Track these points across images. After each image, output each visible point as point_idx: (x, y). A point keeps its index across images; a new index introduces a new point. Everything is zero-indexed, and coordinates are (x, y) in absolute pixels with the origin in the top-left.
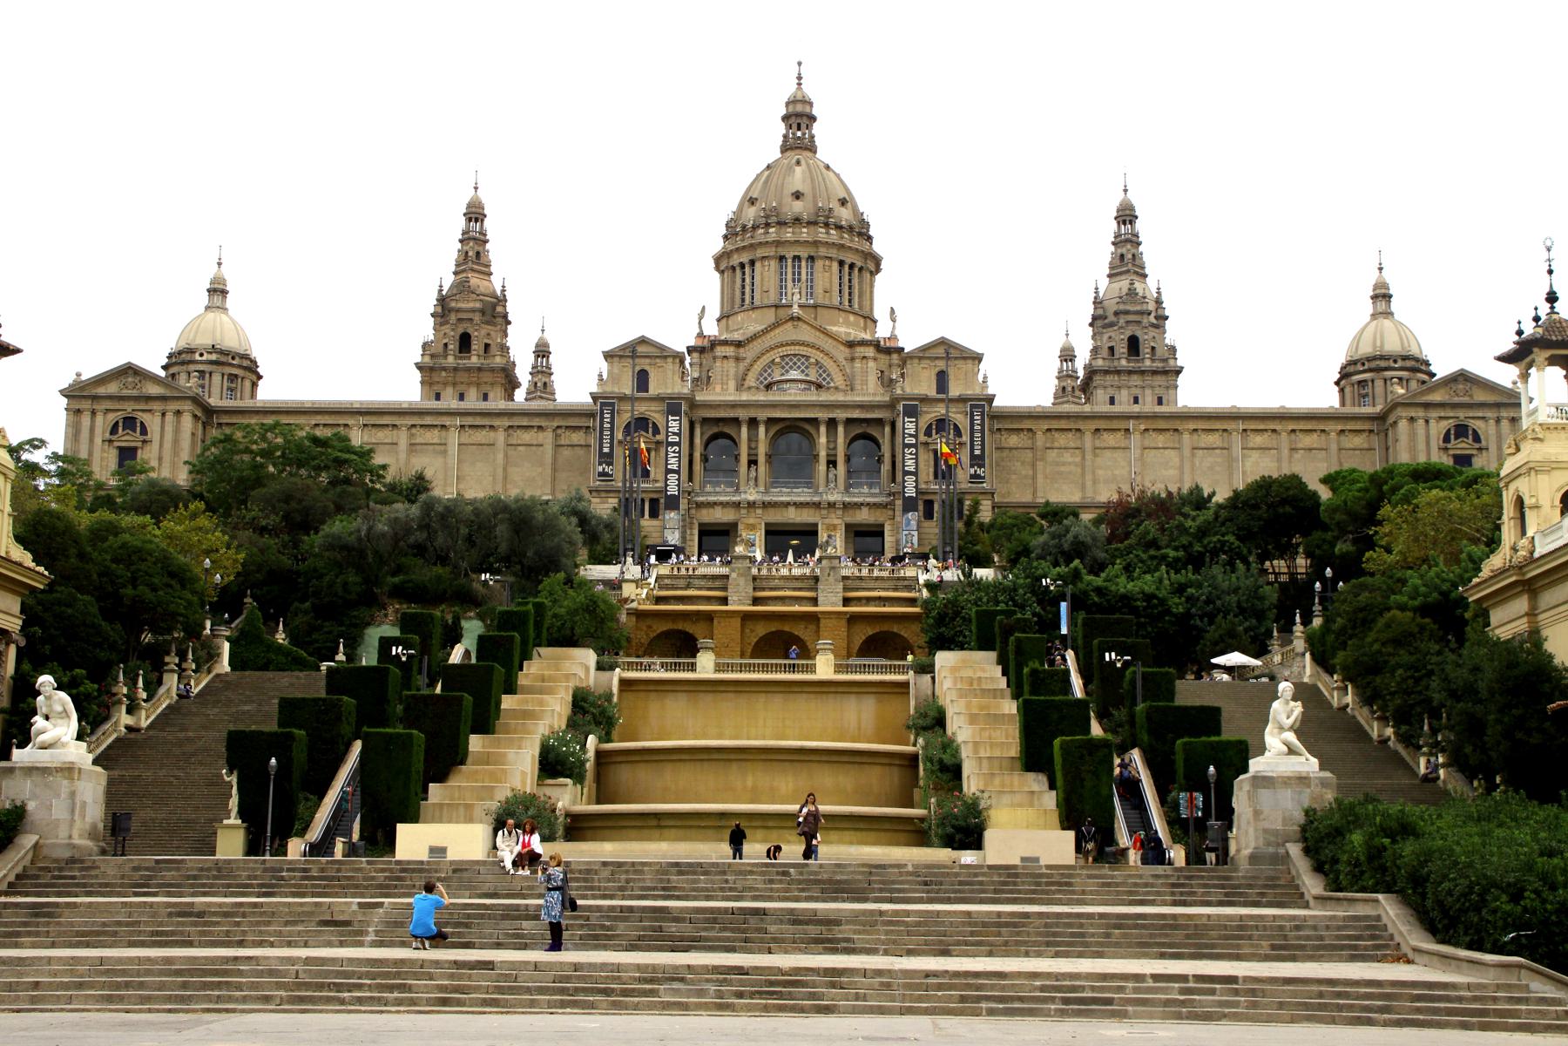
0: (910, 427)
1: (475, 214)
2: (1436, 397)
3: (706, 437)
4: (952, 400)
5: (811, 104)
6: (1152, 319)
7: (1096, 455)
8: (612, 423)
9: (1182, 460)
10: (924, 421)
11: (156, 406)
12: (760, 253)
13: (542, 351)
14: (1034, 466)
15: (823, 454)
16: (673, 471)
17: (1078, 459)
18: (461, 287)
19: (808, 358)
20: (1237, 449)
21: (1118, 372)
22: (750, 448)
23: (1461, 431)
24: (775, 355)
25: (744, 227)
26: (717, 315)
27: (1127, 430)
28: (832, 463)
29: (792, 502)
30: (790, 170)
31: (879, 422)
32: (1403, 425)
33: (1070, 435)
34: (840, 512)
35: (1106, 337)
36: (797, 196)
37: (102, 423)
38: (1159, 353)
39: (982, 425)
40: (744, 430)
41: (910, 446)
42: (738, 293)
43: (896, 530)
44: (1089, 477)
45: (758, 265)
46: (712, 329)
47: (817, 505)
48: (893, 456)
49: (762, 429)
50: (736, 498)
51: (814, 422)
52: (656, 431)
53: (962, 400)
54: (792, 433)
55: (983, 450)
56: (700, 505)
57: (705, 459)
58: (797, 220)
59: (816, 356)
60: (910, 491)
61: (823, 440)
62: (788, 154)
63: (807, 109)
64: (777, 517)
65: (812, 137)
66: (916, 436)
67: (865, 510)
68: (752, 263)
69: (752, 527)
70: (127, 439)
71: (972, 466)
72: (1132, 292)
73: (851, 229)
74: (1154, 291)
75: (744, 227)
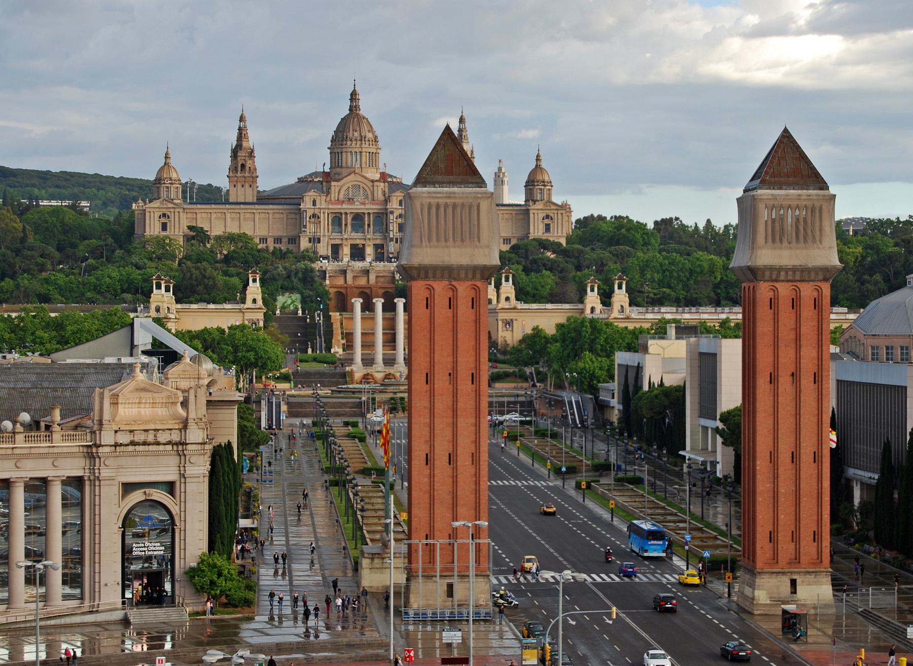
0: (391, 217)
2: (541, 207)
10: (396, 214)
11: (172, 210)
12: (344, 150)
23: (547, 217)
28: (369, 225)
29: (357, 238)
32: (531, 215)
37: (157, 215)
43: (388, 246)
46: (327, 170)
51: (364, 213)
54: (358, 218)
59: (362, 185)
60: (391, 236)
64: (354, 242)
70: (163, 220)
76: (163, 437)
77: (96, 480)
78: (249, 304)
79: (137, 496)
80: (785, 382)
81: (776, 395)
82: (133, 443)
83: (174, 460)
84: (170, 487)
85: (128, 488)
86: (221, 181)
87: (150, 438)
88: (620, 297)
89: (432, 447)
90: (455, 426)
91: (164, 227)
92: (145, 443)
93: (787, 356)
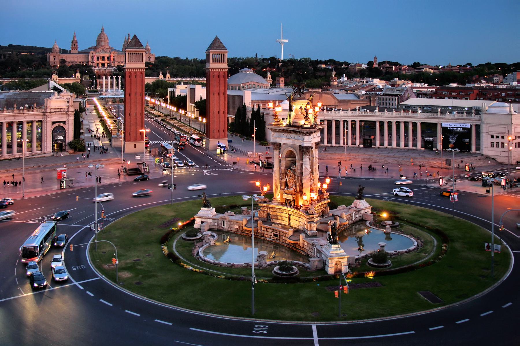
76: (63, 110)
77: (45, 121)
78: (77, 78)
79: (56, 125)
80: (216, 94)
81: (214, 98)
82: (55, 112)
83: (65, 116)
84: (64, 122)
85: (54, 123)
86: (69, 48)
87: (60, 110)
88: (168, 75)
89: (131, 112)
90: (136, 106)
91: (55, 59)
92: (58, 112)
93: (217, 88)
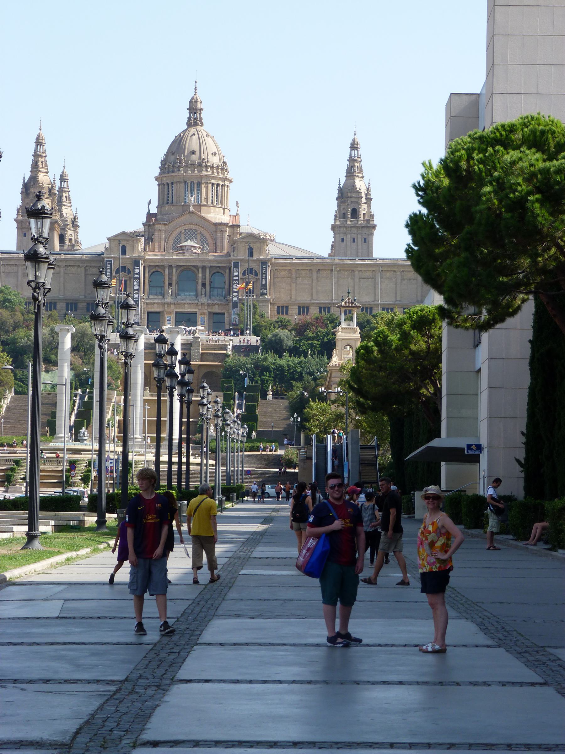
0: (236, 272)
1: (39, 142)
3: (150, 273)
4: (254, 260)
5: (201, 102)
6: (364, 200)
7: (318, 281)
8: (111, 269)
9: (354, 282)
10: (241, 269)
13: (63, 178)
14: (291, 285)
15: (200, 281)
16: (136, 290)
17: (310, 283)
18: (34, 179)
19: (196, 231)
20: (379, 279)
21: (346, 227)
22: (169, 278)
24: (182, 229)
25: (169, 166)
26: (157, 205)
27: (332, 270)
28: (204, 285)
30: (191, 140)
31: (224, 267)
33: (307, 272)
34: (206, 307)
35: (342, 209)
36: (193, 152)
38: (367, 217)
39: (266, 271)
40: (167, 270)
41: (236, 280)
42: (166, 196)
43: (230, 315)
44: (314, 291)
45: (174, 185)
46: (154, 210)
47: (197, 305)
48: (230, 282)
49: (174, 270)
50: (162, 301)
51: (196, 267)
52: (129, 272)
53: (258, 260)
55: (266, 282)
56: (147, 304)
57: (150, 282)
58: (193, 165)
60: (235, 300)
61: (200, 275)
62: (190, 129)
63: (199, 106)
65: (201, 119)
66: (238, 276)
67: (217, 306)
68: (172, 183)
69: (169, 313)
71: (261, 289)
72: (353, 187)
73: (218, 167)
74: (367, 184)
75: (169, 166)
